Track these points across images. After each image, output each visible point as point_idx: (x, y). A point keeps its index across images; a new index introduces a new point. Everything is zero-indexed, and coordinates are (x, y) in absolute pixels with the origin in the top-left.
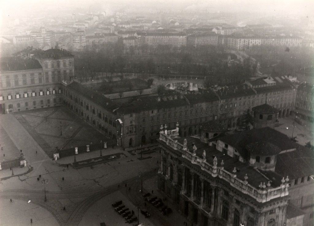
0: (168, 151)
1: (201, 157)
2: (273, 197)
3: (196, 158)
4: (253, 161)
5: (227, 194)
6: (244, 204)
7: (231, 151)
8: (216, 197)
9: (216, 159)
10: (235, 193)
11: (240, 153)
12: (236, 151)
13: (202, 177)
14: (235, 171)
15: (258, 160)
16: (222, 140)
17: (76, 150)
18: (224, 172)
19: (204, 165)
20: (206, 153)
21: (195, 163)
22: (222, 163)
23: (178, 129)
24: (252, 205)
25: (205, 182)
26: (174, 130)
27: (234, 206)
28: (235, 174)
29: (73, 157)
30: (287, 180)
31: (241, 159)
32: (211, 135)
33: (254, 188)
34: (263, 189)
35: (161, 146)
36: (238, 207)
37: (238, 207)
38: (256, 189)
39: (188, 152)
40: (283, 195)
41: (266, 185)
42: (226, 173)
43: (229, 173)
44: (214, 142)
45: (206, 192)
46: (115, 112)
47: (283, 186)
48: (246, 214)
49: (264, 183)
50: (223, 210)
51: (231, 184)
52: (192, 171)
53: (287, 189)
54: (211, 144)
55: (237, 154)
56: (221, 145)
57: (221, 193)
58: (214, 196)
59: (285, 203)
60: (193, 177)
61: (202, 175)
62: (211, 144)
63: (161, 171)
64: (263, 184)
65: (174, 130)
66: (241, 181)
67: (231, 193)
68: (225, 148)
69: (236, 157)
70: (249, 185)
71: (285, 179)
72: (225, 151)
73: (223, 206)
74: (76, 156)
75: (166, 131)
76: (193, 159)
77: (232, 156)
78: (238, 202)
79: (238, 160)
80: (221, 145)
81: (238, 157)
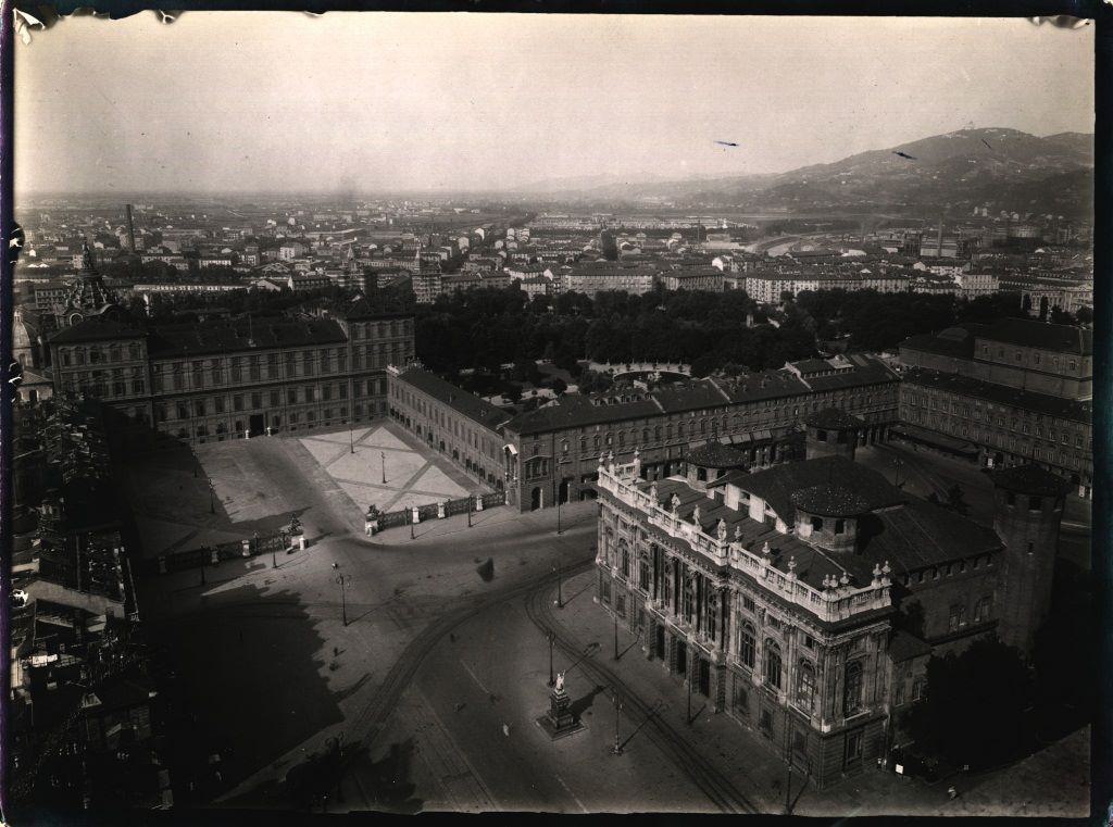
0: (616, 511)
1: (693, 523)
2: (855, 611)
3: (679, 523)
4: (805, 530)
5: (750, 604)
6: (790, 627)
7: (758, 509)
8: (725, 612)
9: (722, 524)
10: (769, 601)
11: (777, 512)
12: (768, 508)
13: (693, 568)
14: (766, 550)
15: (817, 525)
16: (737, 484)
17: (416, 515)
18: (743, 554)
19: (696, 539)
20: (700, 511)
21: (677, 536)
22: (737, 534)
23: (636, 462)
24: (809, 629)
25: (699, 577)
26: (628, 465)
27: (766, 631)
28: (767, 557)
29: (409, 527)
30: (886, 569)
31: (781, 528)
32: (712, 477)
33: (811, 590)
34: (830, 590)
35: (601, 500)
36: (777, 635)
37: (777, 635)
38: (815, 591)
39: (661, 510)
40: (877, 605)
41: (838, 580)
42: (746, 556)
43: (755, 557)
44: (719, 490)
45: (703, 603)
46: (501, 429)
47: (874, 585)
48: (796, 651)
49: (834, 576)
50: (742, 642)
51: (760, 581)
52: (671, 553)
53: (886, 593)
54: (711, 495)
55: (772, 513)
56: (733, 497)
57: (736, 605)
58: (720, 612)
59: (885, 626)
60: (672, 568)
61: (691, 562)
62: (711, 495)
63: (601, 558)
64: (831, 579)
65: (628, 465)
66: (782, 574)
67: (759, 602)
68: (745, 501)
69: (770, 522)
70: (800, 582)
71: (880, 568)
72: (744, 509)
73: (743, 633)
74: (415, 527)
75: (612, 467)
76: (672, 524)
77: (760, 519)
78: (774, 622)
79: (773, 527)
80: (733, 497)
81: (775, 520)
